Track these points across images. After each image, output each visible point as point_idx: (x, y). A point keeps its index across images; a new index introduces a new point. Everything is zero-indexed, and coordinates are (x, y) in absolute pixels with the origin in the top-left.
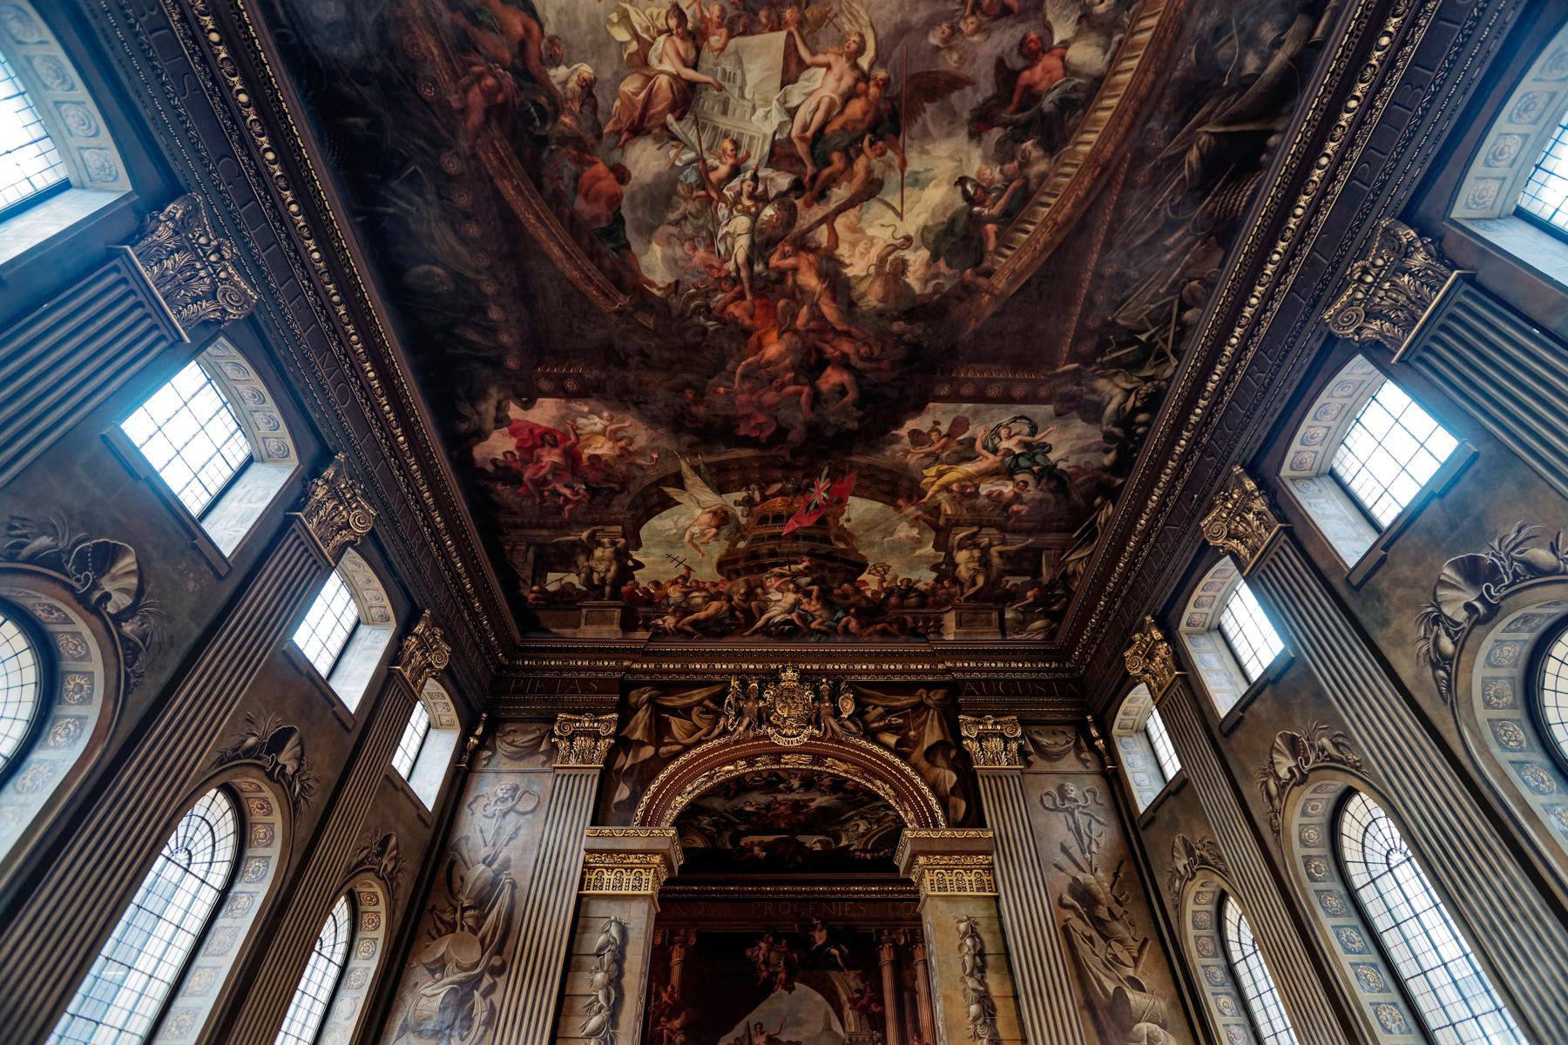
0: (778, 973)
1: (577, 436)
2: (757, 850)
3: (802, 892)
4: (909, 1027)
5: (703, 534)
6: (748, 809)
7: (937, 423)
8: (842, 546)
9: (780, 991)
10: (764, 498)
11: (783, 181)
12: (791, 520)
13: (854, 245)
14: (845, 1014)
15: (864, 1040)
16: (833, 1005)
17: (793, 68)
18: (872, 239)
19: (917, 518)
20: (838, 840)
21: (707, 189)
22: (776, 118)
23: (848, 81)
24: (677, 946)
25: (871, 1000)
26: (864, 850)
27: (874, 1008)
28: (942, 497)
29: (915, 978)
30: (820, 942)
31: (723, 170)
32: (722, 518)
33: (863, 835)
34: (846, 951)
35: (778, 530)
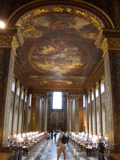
1: (95, 36)
5: (79, 21)
7: (37, 36)
8: (49, 18)
10: (65, 27)
11: (60, 52)
12: (60, 23)
13: (53, 49)
17: (60, 56)
18: (51, 49)
19: (34, 23)
21: (69, 52)
22: (61, 55)
23: (55, 56)
28: (30, 26)
31: (67, 53)
32: (74, 24)
35: (63, 21)
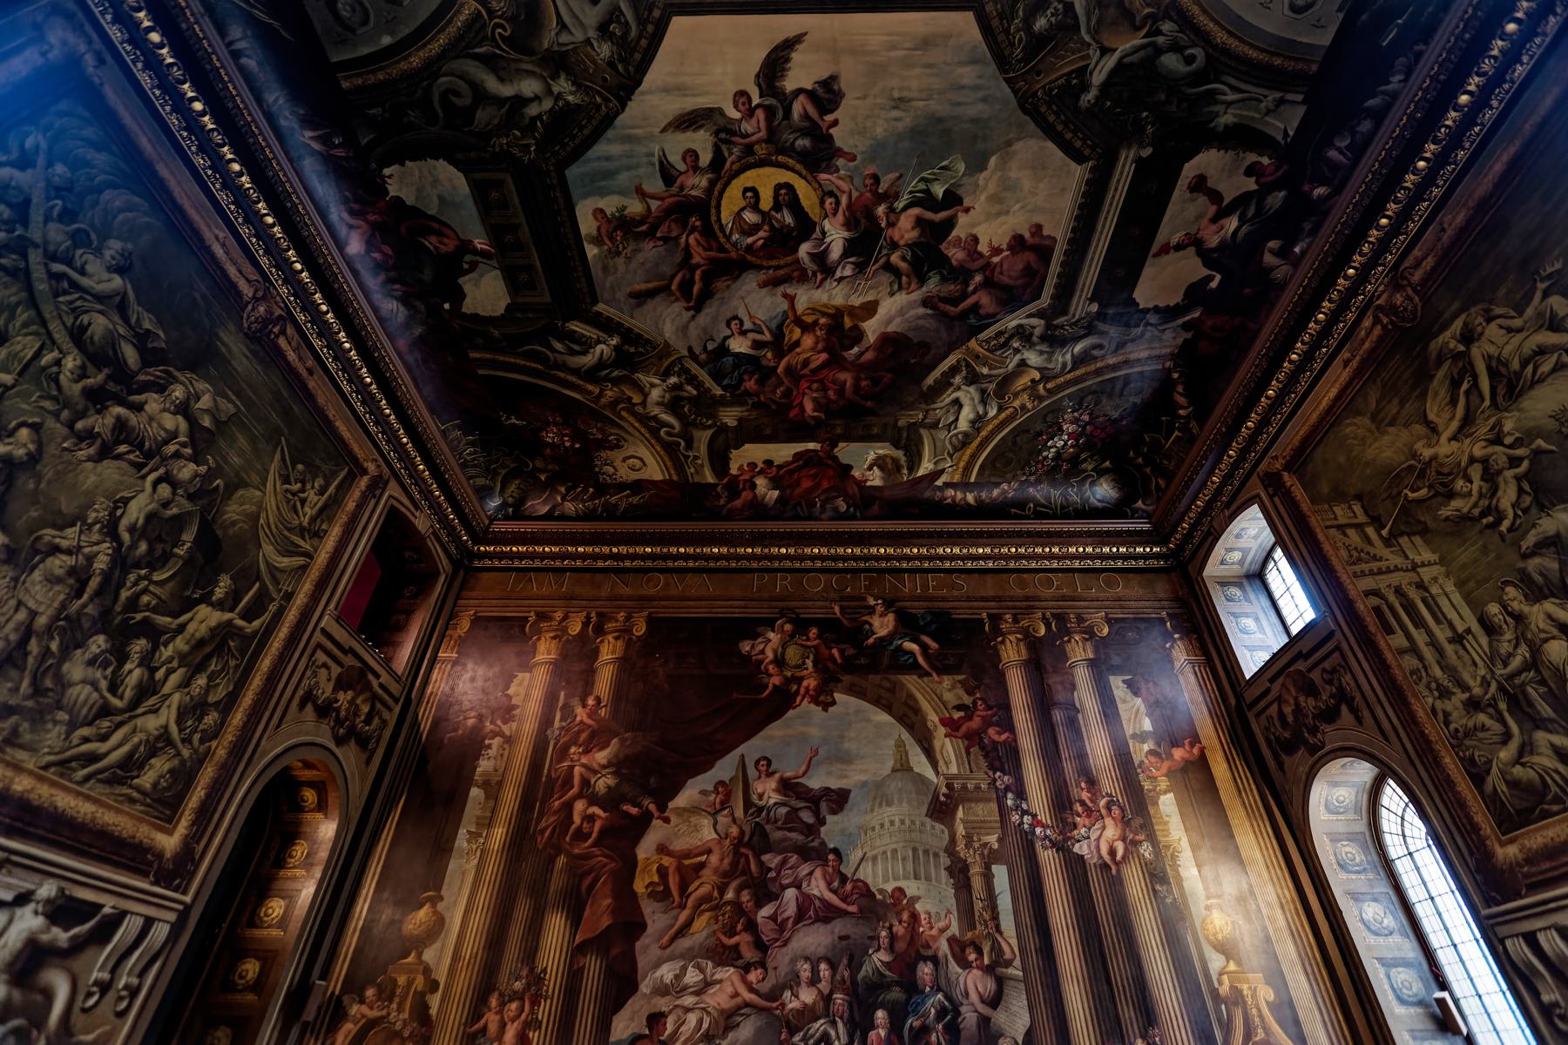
0: (801, 679)
2: (761, 482)
3: (845, 558)
4: (1069, 769)
6: (739, 345)
9: (806, 705)
14: (937, 744)
15: (978, 788)
16: (910, 728)
20: (914, 460)
24: (610, 637)
25: (987, 723)
26: (964, 485)
29: (1073, 687)
30: (882, 632)
33: (966, 440)
34: (934, 645)
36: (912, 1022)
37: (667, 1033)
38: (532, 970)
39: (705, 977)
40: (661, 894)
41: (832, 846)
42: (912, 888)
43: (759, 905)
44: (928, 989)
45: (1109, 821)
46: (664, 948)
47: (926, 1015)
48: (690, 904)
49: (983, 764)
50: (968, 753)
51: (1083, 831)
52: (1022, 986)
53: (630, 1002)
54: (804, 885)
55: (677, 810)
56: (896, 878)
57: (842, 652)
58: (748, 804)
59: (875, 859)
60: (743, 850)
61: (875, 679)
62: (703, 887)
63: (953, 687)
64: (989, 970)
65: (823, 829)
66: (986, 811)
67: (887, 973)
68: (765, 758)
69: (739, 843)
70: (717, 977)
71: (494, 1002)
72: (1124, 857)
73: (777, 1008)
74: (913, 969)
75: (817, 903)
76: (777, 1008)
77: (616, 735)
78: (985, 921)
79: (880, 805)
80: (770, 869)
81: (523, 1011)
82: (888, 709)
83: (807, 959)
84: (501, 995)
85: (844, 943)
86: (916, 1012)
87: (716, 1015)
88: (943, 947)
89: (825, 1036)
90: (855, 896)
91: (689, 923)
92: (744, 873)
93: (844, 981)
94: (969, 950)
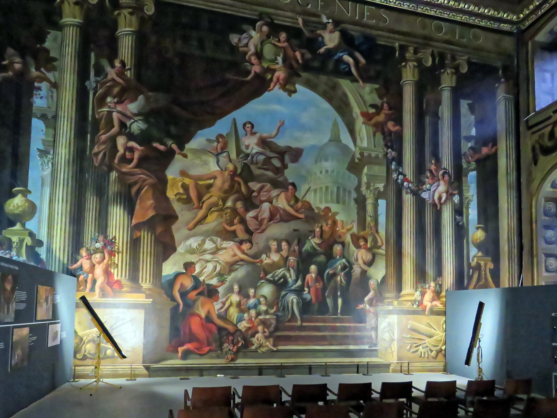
27: (390, 125)
34: (362, 60)
36: (329, 271)
37: (196, 272)
38: (106, 237)
39: (216, 247)
40: (188, 201)
41: (291, 181)
42: (334, 208)
43: (247, 210)
44: (338, 257)
45: (442, 182)
46: (190, 229)
47: (336, 268)
48: (205, 206)
49: (382, 142)
50: (374, 135)
51: (428, 186)
52: (384, 257)
53: (172, 256)
54: (274, 201)
55: (196, 152)
56: (327, 202)
57: (303, 55)
58: (239, 151)
59: (315, 191)
60: (236, 179)
61: (323, 78)
62: (213, 197)
63: (371, 92)
64: (369, 250)
65: (286, 171)
66: (380, 170)
67: (319, 249)
68: (250, 123)
69: (234, 174)
70: (224, 246)
71: (83, 252)
72: (445, 201)
73: (258, 262)
74: (331, 247)
75: (281, 212)
76: (258, 262)
77: (142, 93)
78: (371, 227)
79: (321, 161)
80: (254, 191)
81: (104, 258)
82: (330, 100)
83: (275, 240)
84: (88, 250)
85: (296, 233)
86: (331, 267)
87: (224, 264)
88: (348, 239)
89: (284, 276)
90: (303, 210)
91: (205, 217)
92: (237, 192)
93: (294, 251)
94: (360, 240)
